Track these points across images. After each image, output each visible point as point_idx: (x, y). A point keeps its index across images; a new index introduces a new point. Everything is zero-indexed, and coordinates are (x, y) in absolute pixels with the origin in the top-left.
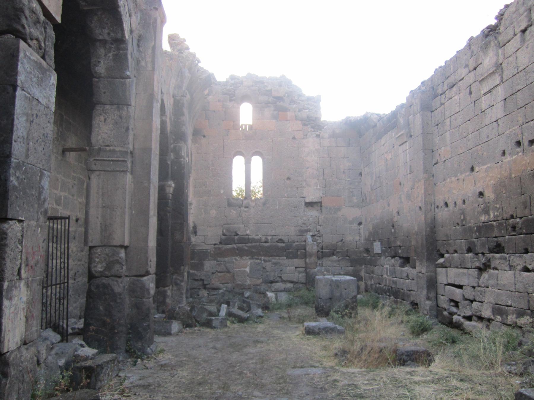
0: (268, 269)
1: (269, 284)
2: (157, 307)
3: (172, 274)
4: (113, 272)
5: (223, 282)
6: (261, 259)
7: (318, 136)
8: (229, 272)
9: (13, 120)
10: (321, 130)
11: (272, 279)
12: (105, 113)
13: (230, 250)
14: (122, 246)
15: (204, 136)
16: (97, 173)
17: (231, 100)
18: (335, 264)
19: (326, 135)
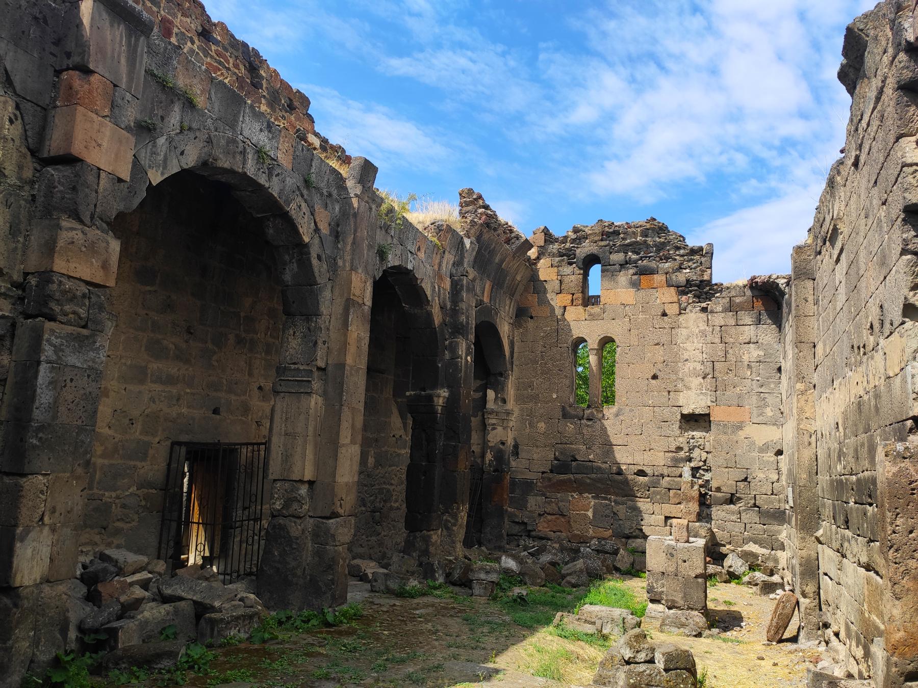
0: (621, 515)
1: (623, 540)
2: (419, 556)
3: (443, 513)
4: (291, 511)
5: (554, 529)
6: (610, 500)
7: (704, 310)
8: (563, 515)
9: (35, 391)
10: (710, 300)
11: (627, 532)
12: (295, 326)
13: (563, 482)
14: (301, 481)
15: (532, 318)
16: (282, 394)
17: (570, 264)
18: (734, 518)
19: (719, 309)
